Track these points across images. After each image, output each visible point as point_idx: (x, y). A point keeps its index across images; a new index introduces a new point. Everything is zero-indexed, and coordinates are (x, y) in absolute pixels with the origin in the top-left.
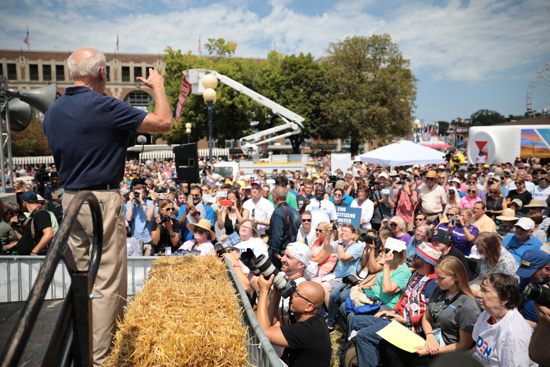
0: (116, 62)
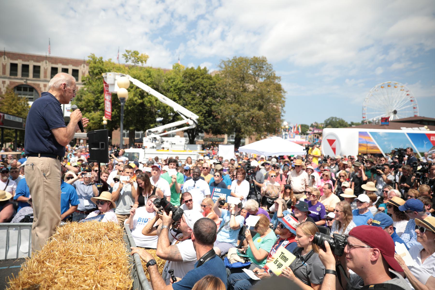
0: (46, 63)
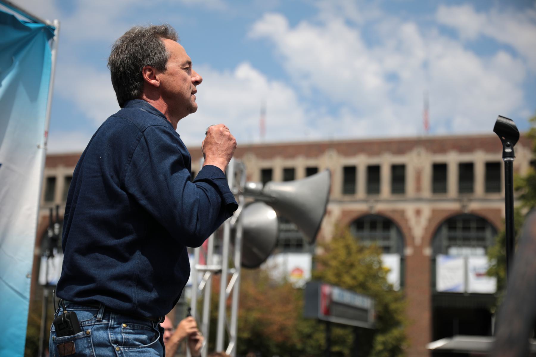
0: (419, 155)
